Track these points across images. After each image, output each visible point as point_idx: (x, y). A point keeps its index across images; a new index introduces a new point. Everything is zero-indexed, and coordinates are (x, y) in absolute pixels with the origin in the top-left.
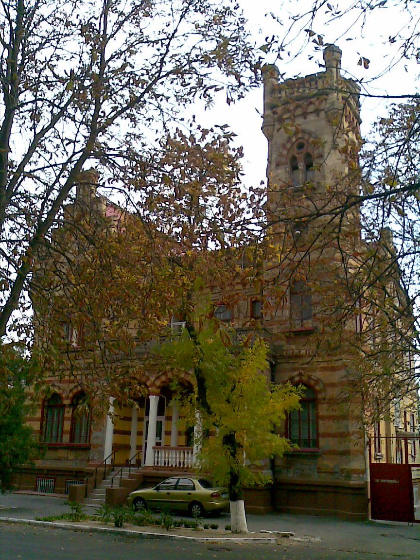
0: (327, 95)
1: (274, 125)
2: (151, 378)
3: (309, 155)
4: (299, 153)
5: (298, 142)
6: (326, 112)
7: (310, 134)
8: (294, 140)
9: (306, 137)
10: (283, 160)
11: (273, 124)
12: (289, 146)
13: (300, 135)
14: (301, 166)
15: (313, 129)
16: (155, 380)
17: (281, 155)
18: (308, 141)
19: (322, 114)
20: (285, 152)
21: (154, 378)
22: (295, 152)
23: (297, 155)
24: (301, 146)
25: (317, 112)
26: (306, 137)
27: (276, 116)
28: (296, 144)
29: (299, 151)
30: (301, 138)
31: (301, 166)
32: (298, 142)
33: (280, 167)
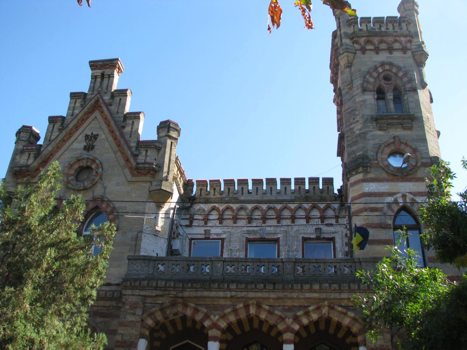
0: (412, 38)
1: (355, 53)
2: (212, 317)
3: (396, 89)
4: (386, 84)
5: (384, 73)
6: (412, 52)
7: (399, 68)
8: (380, 70)
9: (394, 70)
10: (370, 87)
11: (354, 52)
12: (375, 74)
13: (387, 67)
14: (390, 96)
15: (401, 65)
16: (218, 320)
17: (365, 81)
18: (396, 74)
19: (409, 53)
20: (372, 80)
21: (217, 317)
22: (383, 82)
23: (384, 85)
24: (387, 78)
25: (404, 50)
26: (394, 70)
27: (357, 46)
28: (382, 75)
29: (387, 82)
30: (387, 70)
31: (390, 96)
32: (384, 73)
33: (367, 93)
